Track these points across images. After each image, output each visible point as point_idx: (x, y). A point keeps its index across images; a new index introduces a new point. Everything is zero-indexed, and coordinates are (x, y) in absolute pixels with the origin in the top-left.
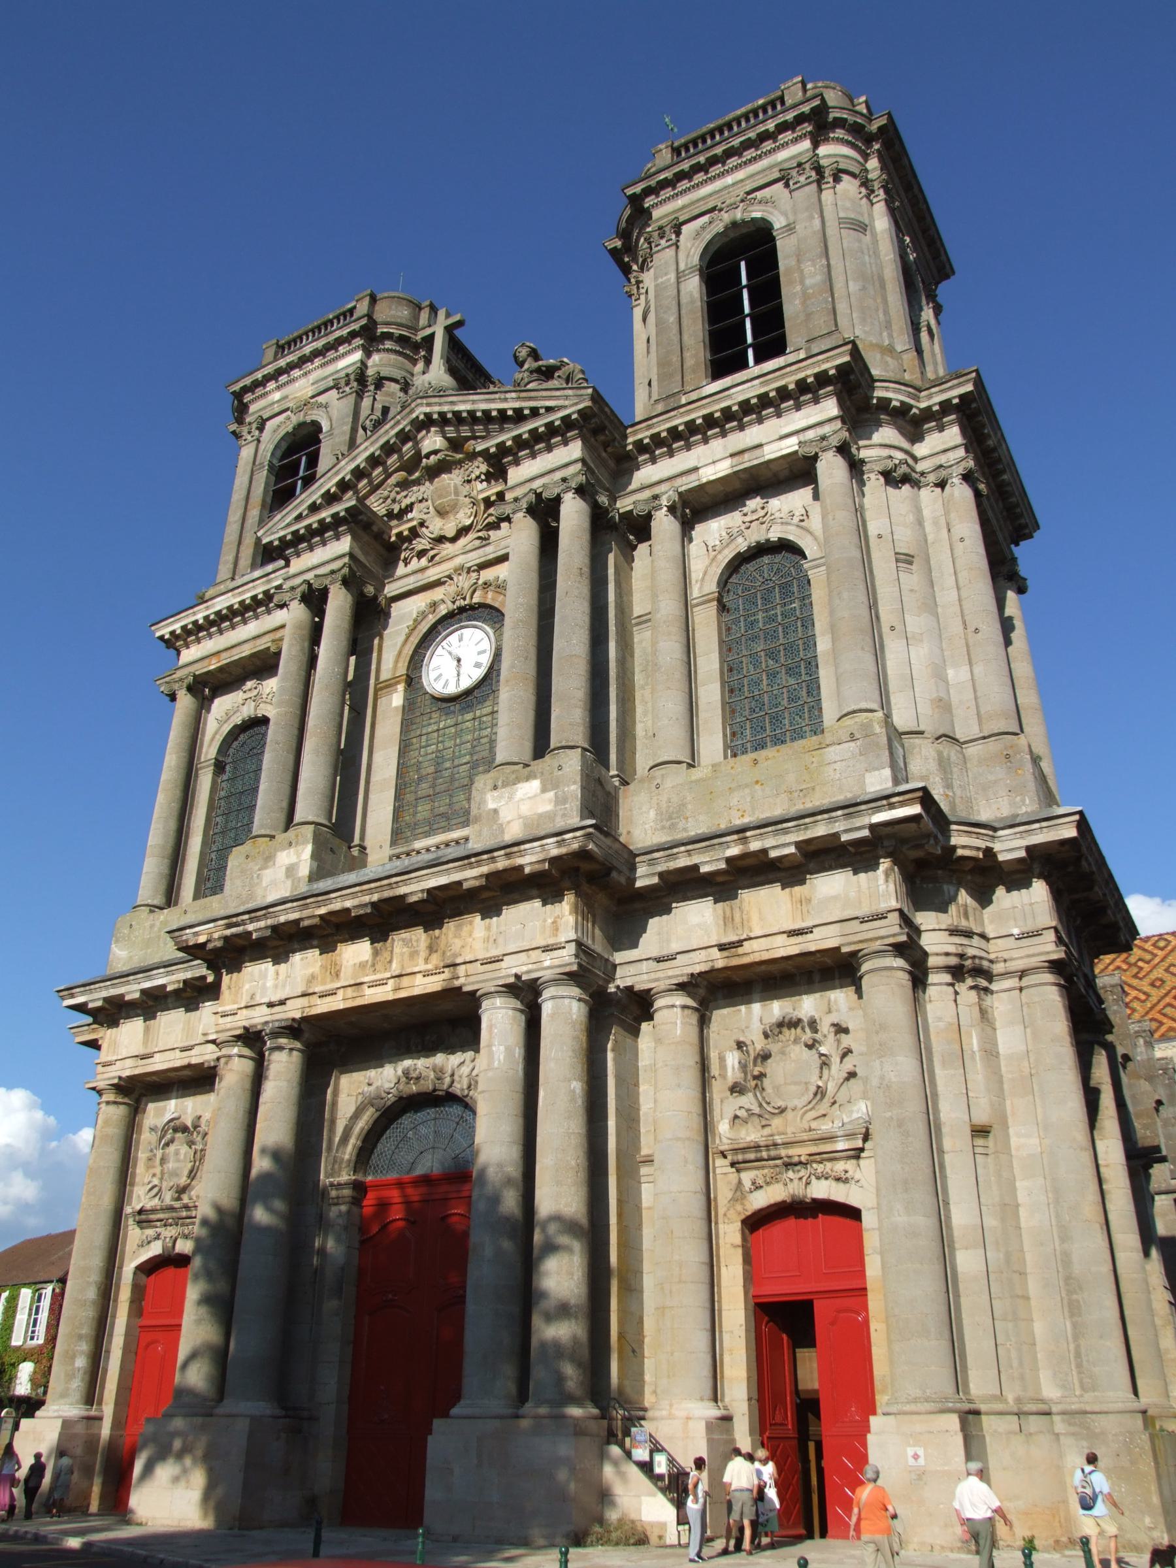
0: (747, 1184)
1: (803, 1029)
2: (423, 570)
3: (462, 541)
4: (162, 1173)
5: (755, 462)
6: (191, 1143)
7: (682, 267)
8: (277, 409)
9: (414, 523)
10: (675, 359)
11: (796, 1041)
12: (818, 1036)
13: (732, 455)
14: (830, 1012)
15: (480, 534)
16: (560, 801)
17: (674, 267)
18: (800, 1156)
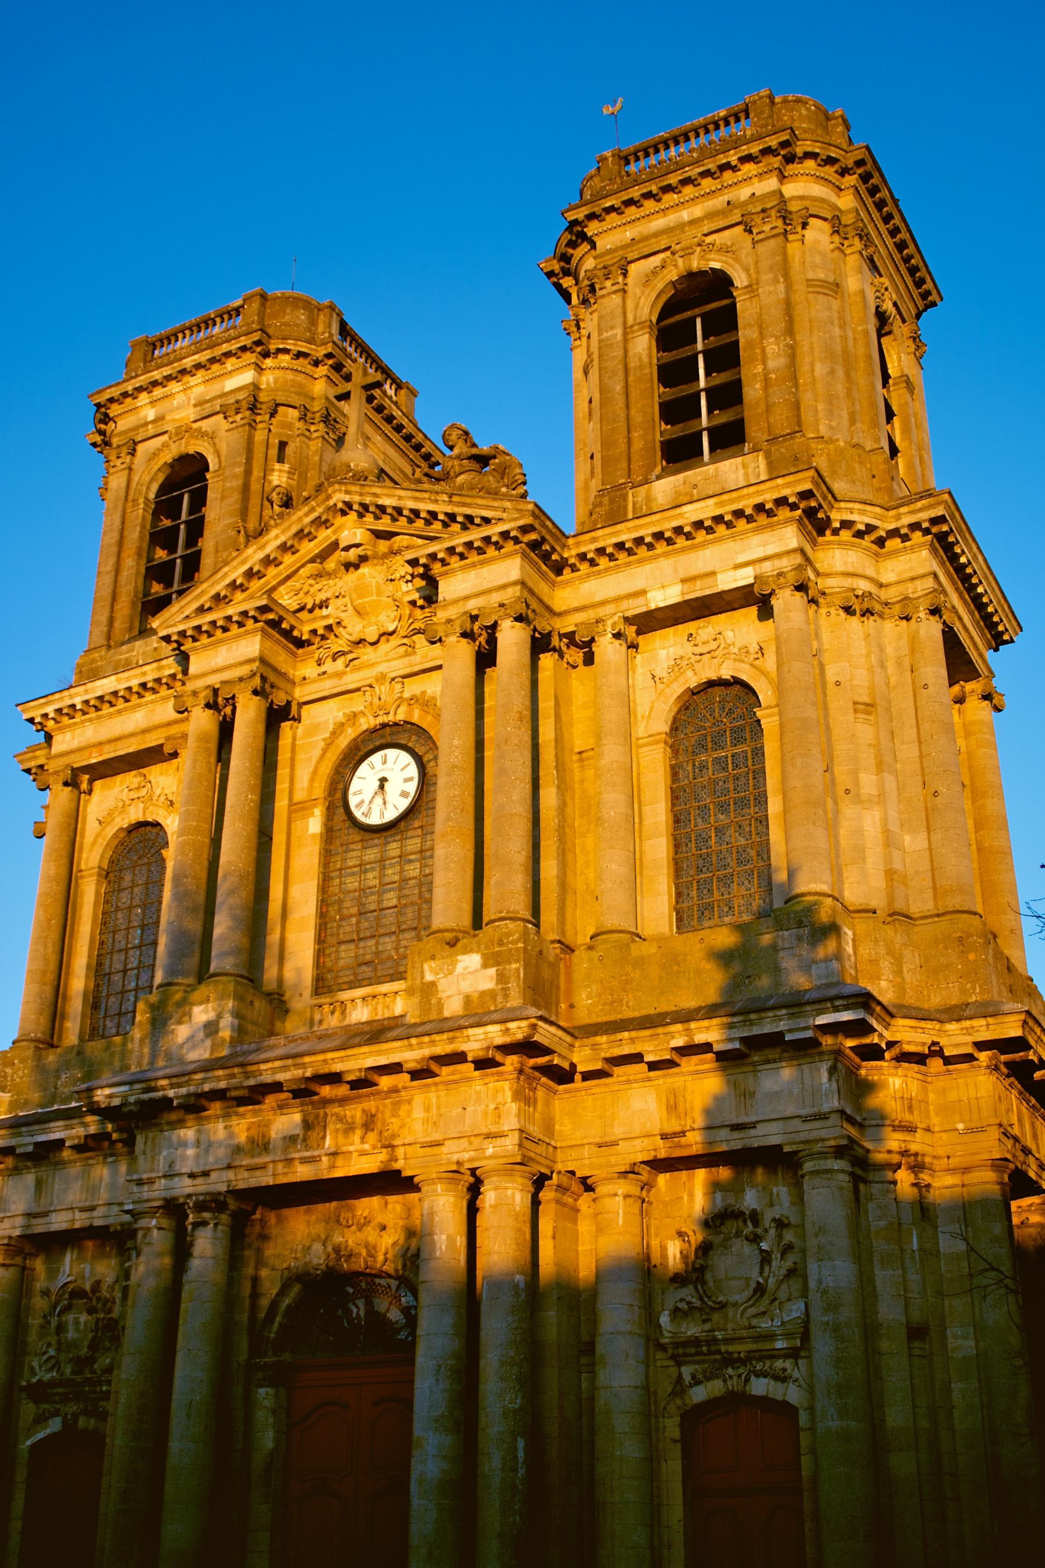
0: (687, 1378)
1: (745, 1221)
2: (339, 675)
3: (384, 647)
4: (59, 1342)
5: (708, 592)
6: (91, 1311)
7: (630, 321)
8: (151, 430)
9: (330, 621)
10: (622, 439)
11: (738, 1234)
12: (759, 1231)
13: (683, 581)
14: (772, 1205)
15: (405, 641)
16: (501, 978)
17: (620, 320)
18: (739, 1353)
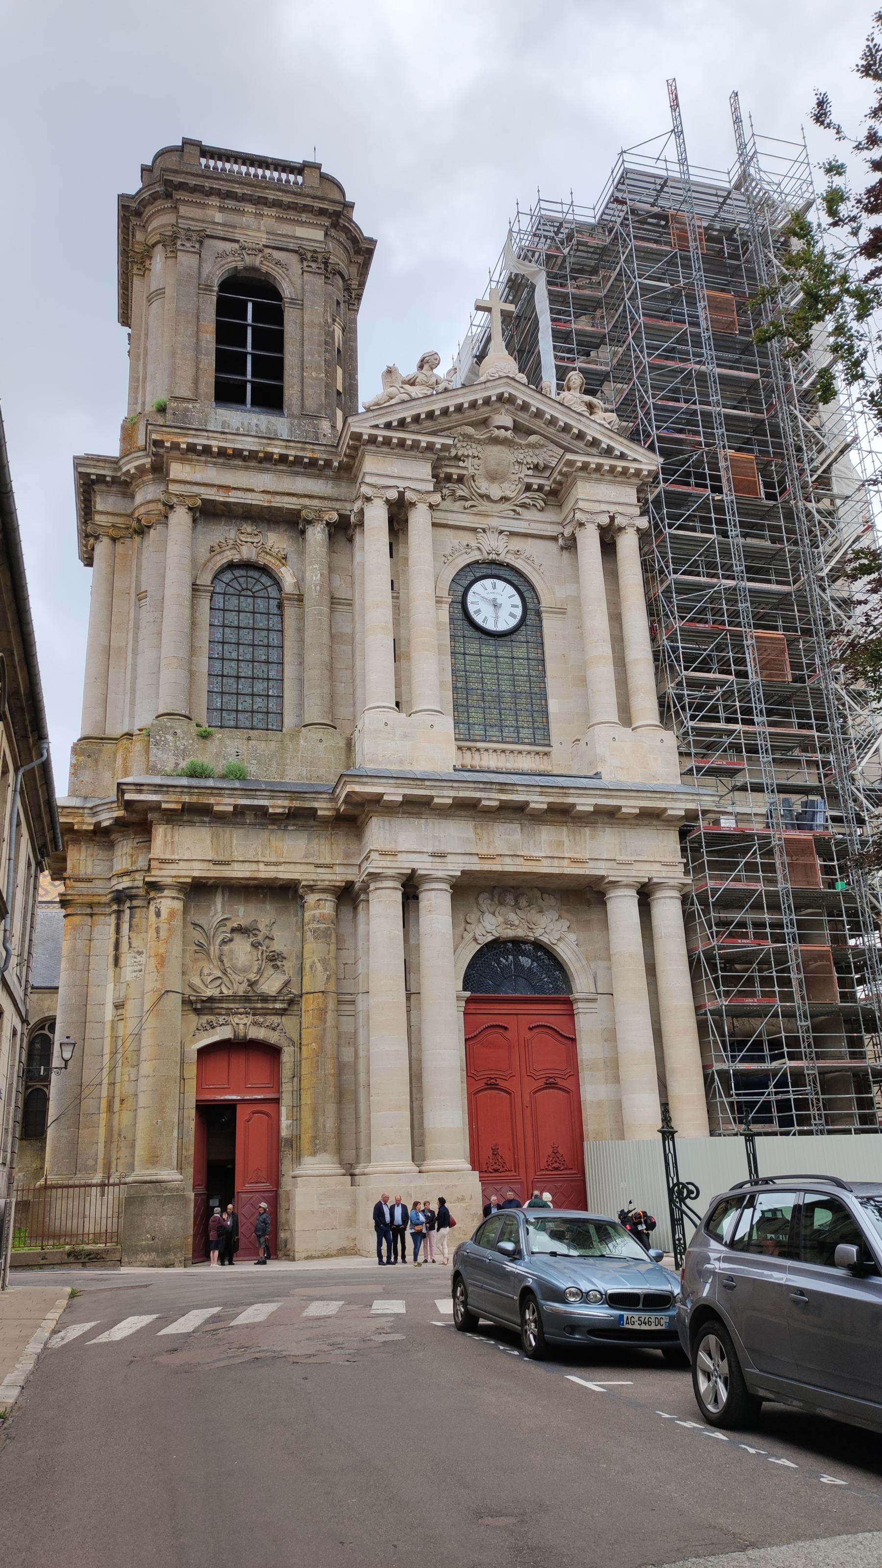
8: (221, 234)
9: (465, 472)
